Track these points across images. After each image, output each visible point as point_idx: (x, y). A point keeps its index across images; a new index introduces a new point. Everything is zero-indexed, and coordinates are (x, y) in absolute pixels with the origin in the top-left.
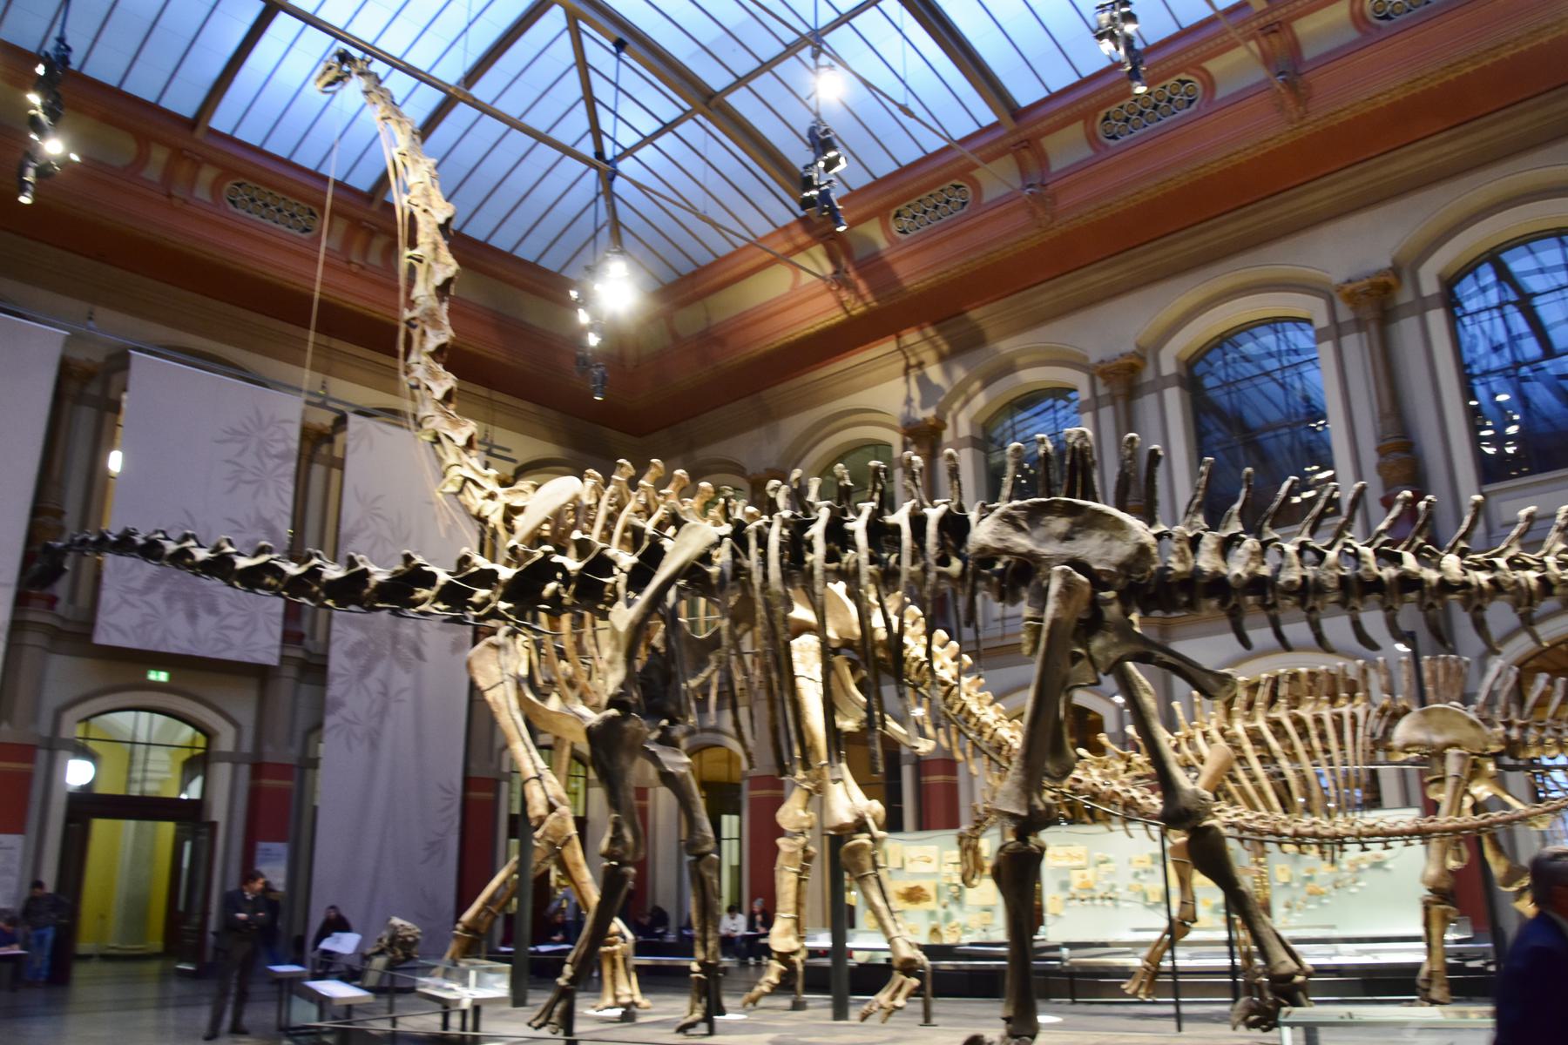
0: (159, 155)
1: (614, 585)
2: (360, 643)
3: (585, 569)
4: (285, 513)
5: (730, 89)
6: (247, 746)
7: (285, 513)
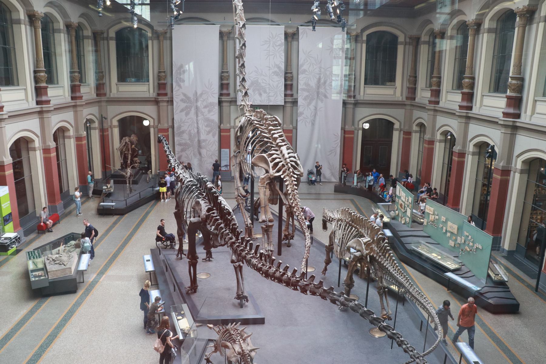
2: (307, 96)
4: (283, 62)
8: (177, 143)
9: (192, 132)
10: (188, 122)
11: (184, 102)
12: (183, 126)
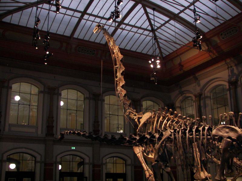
0: (64, 44)
1: (156, 140)
3: (150, 137)
5: (179, 13)
6: (91, 161)
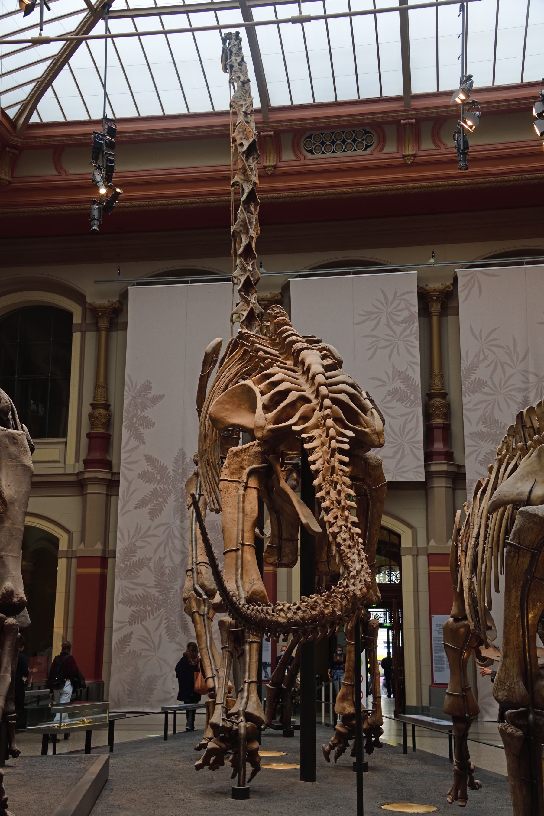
4: (415, 363)
7: (415, 363)
8: (121, 597)
9: (167, 563)
10: (155, 536)
11: (149, 481)
12: (143, 547)
